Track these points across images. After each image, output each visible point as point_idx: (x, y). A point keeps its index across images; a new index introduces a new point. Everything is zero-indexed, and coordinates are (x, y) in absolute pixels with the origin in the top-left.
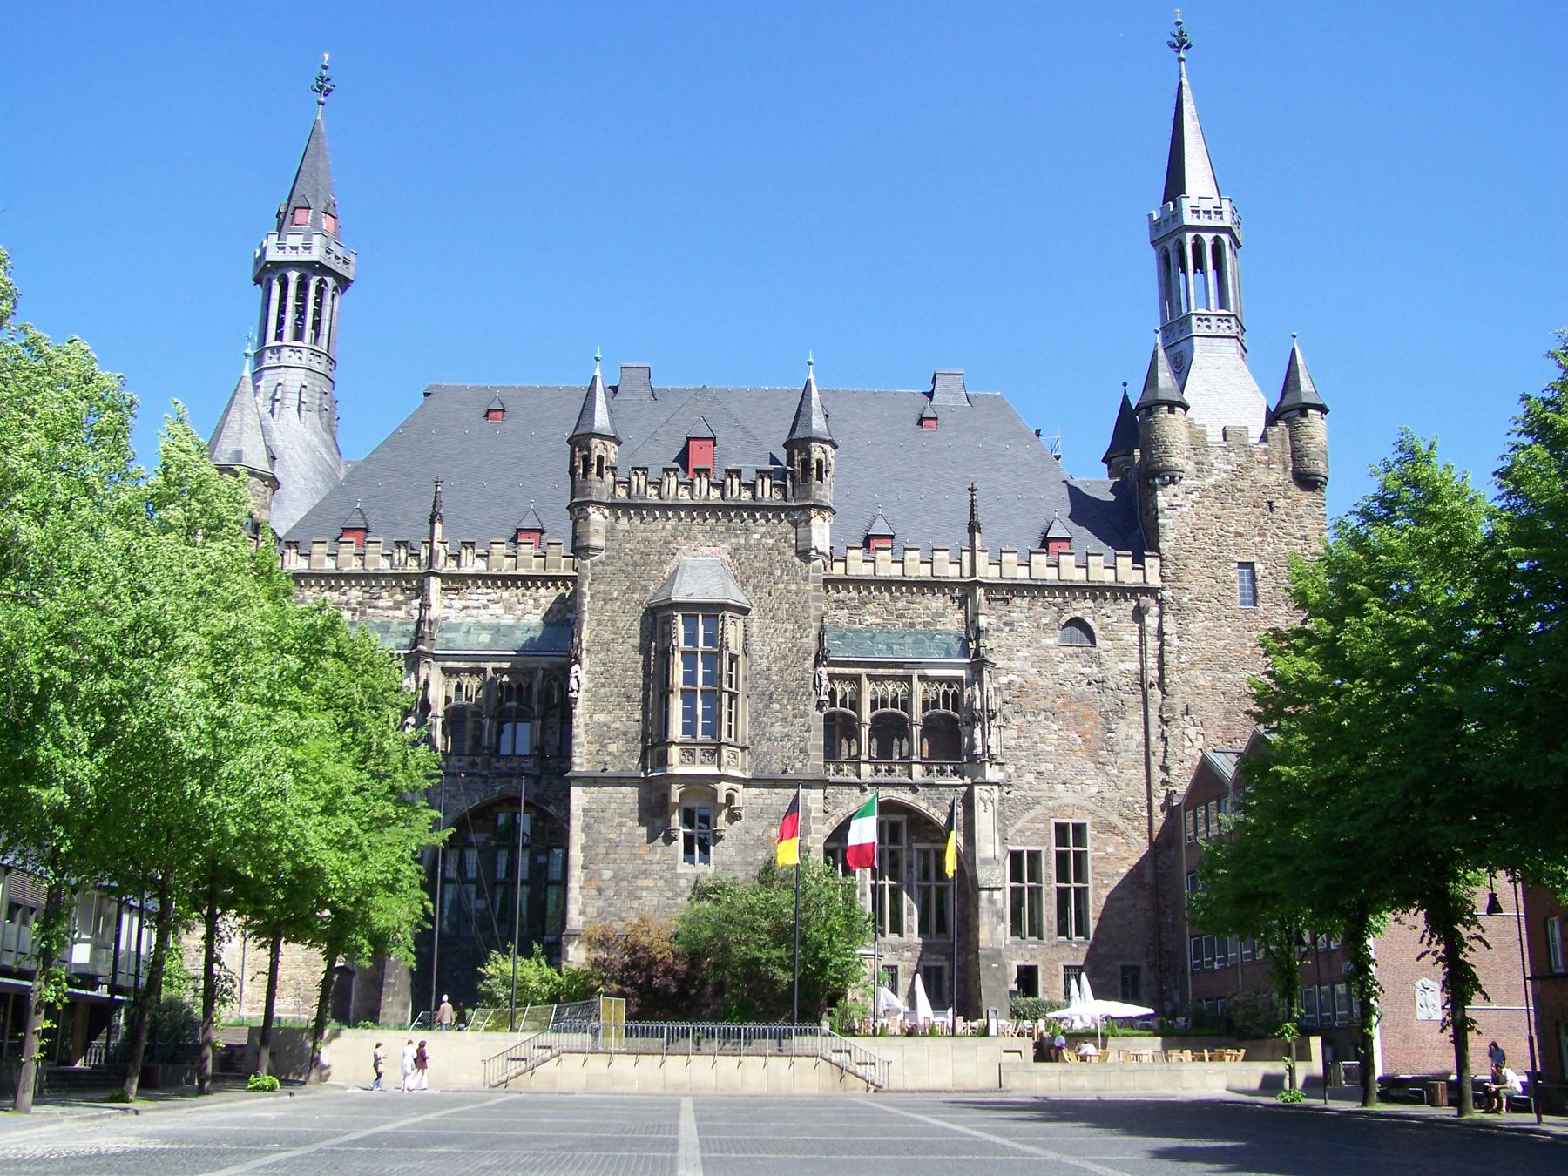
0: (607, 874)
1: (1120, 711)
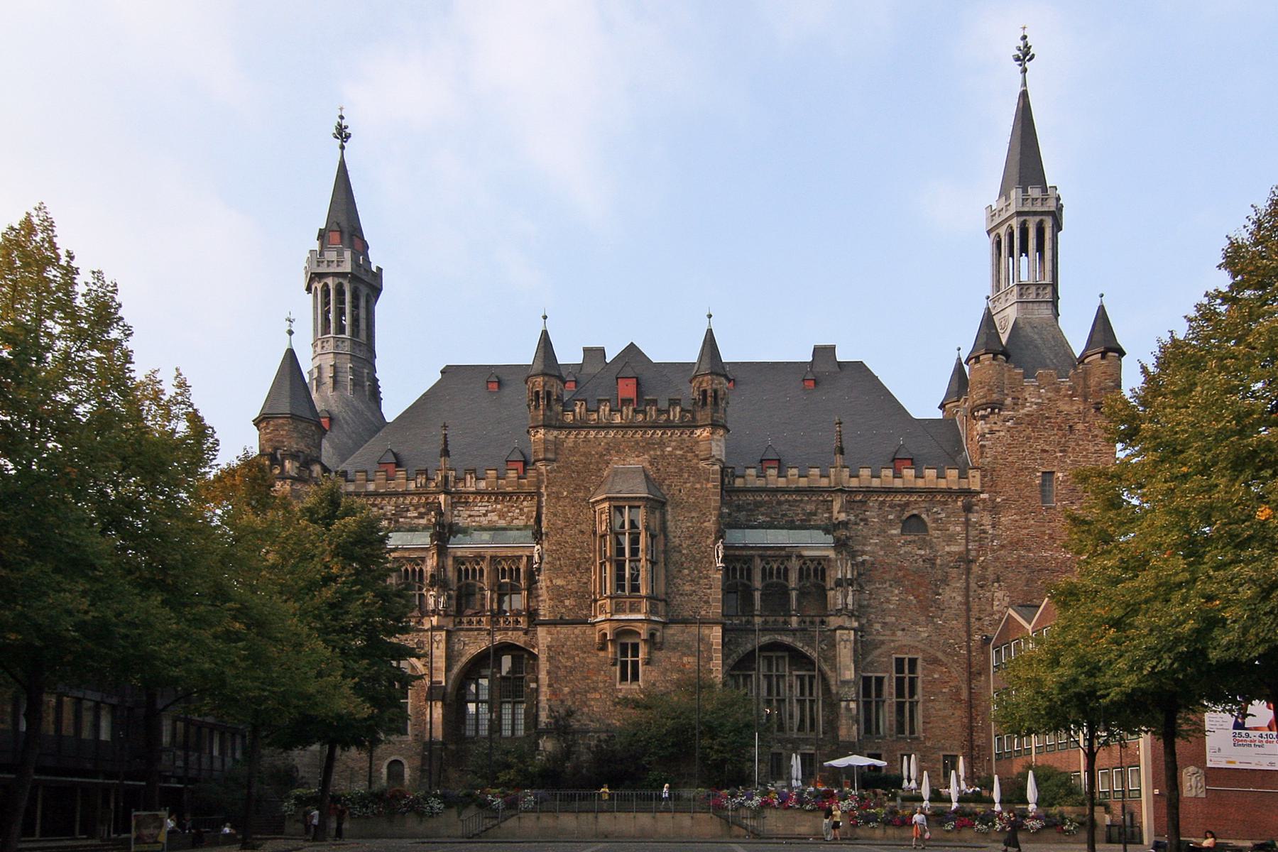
1: (945, 581)
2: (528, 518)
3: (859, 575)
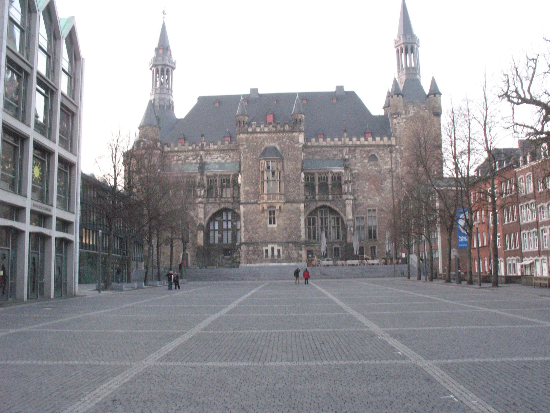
0: (250, 228)
1: (385, 179)
2: (233, 159)
3: (353, 178)
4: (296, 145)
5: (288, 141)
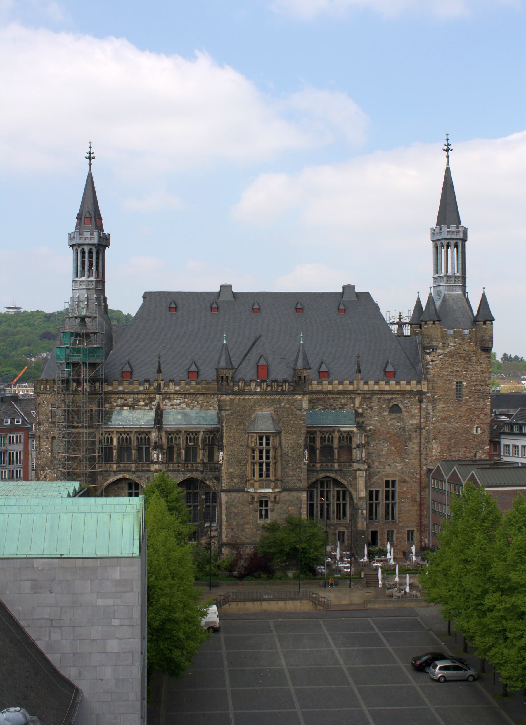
0: (234, 523)
1: (410, 439)
2: (202, 406)
4: (298, 412)
5: (288, 406)
